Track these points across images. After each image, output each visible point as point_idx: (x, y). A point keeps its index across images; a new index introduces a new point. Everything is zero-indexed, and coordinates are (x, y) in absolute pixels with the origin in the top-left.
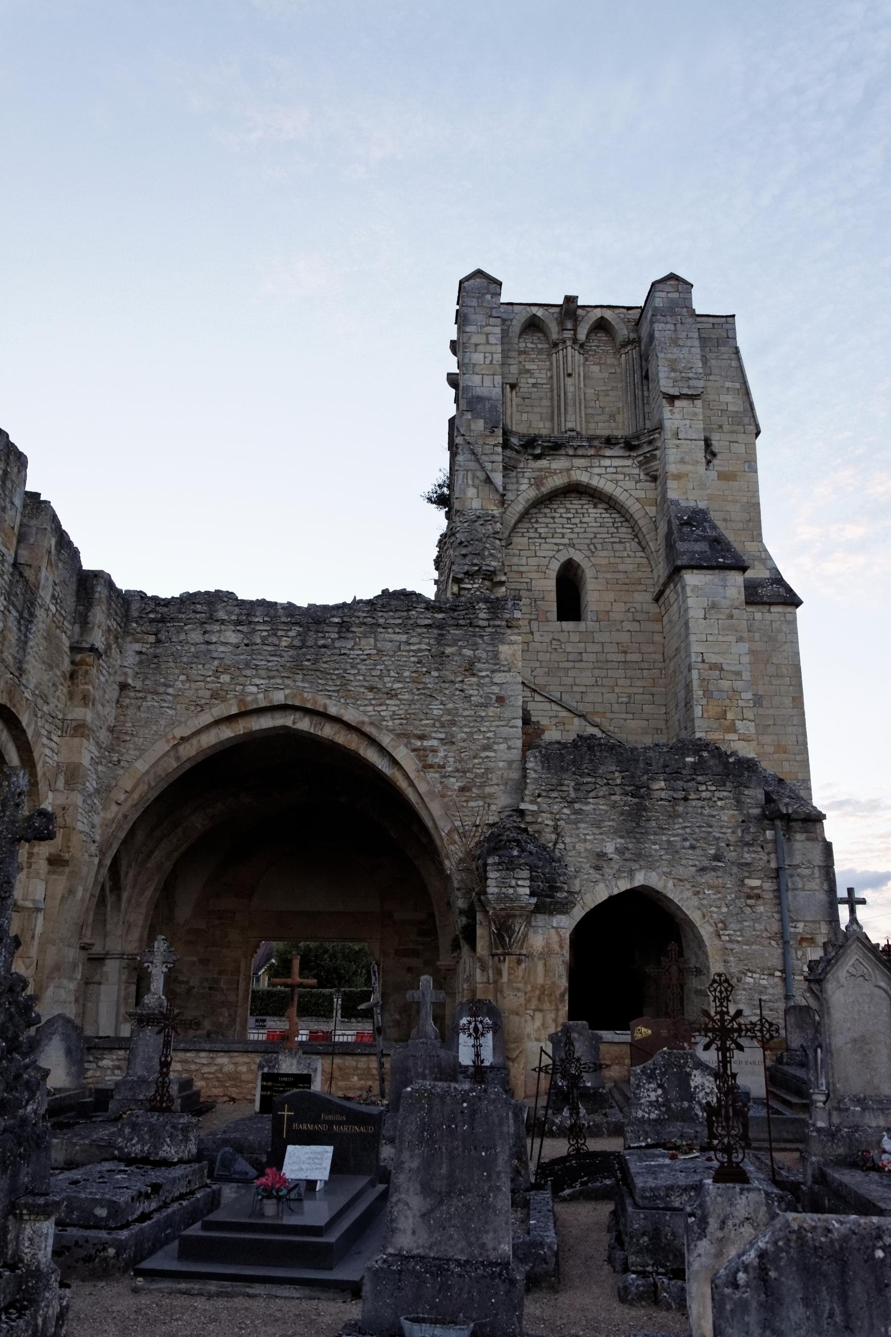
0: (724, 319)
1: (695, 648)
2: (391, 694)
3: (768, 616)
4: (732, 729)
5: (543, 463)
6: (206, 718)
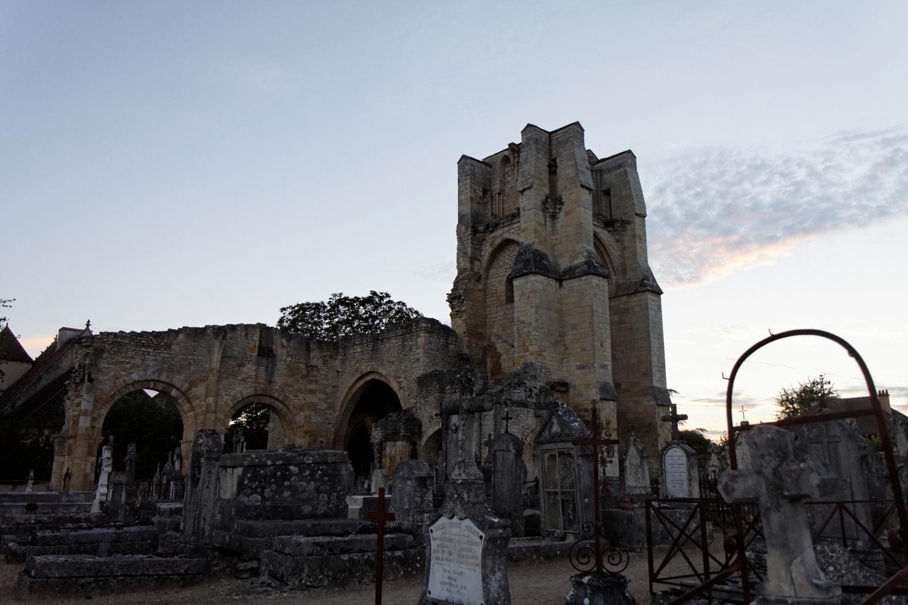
1: (516, 315)
2: (393, 363)
3: (580, 283)
4: (527, 350)
5: (494, 234)
6: (354, 379)
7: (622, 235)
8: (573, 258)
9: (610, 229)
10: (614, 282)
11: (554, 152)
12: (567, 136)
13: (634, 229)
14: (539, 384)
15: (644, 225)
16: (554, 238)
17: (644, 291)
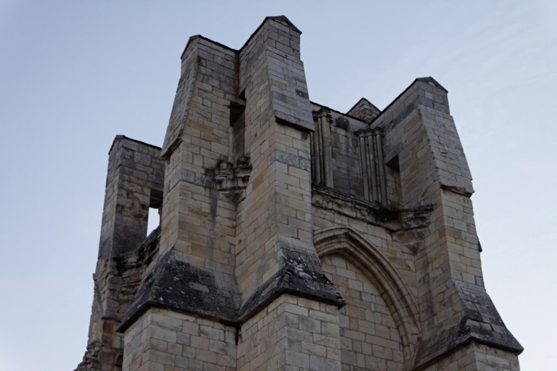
0: (262, 28)
3: (268, 319)
7: (421, 236)
8: (262, 270)
9: (393, 226)
10: (413, 339)
11: (242, 80)
12: (260, 42)
13: (440, 219)
15: (469, 211)
16: (235, 241)
17: (465, 345)
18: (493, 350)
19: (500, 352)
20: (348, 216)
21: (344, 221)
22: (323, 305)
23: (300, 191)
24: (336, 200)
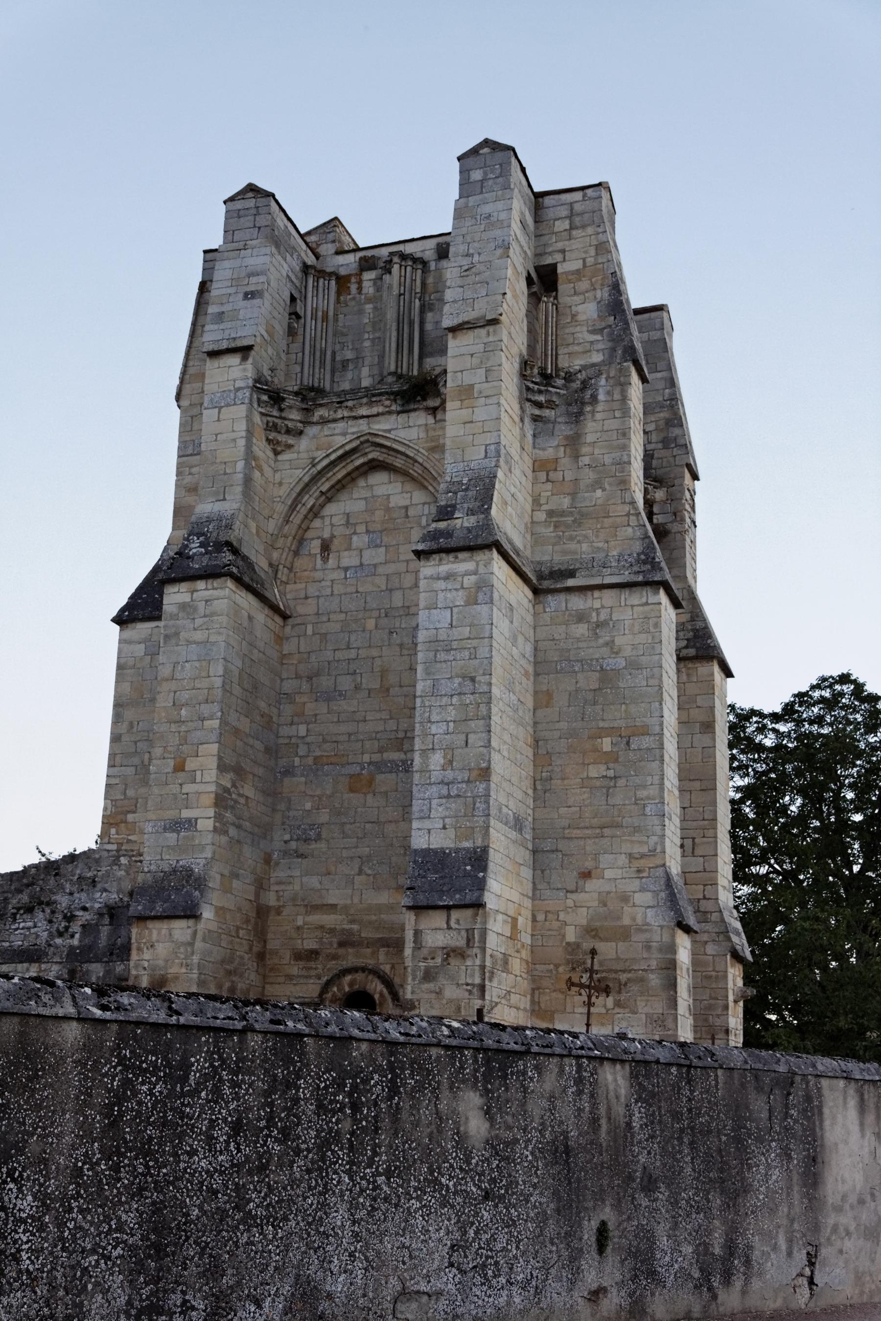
14: (99, 899)
18: (451, 557)
19: (461, 555)
20: (368, 417)
21: (363, 426)
22: (210, 581)
23: (234, 435)
24: (345, 404)
